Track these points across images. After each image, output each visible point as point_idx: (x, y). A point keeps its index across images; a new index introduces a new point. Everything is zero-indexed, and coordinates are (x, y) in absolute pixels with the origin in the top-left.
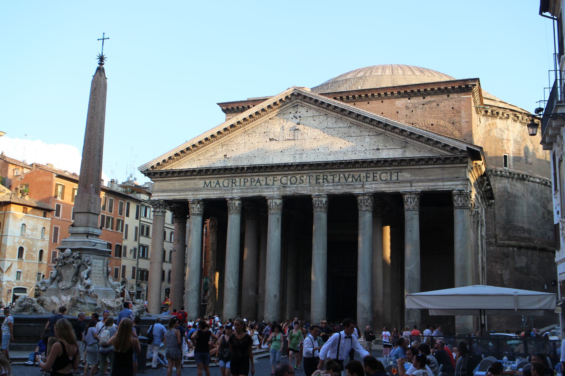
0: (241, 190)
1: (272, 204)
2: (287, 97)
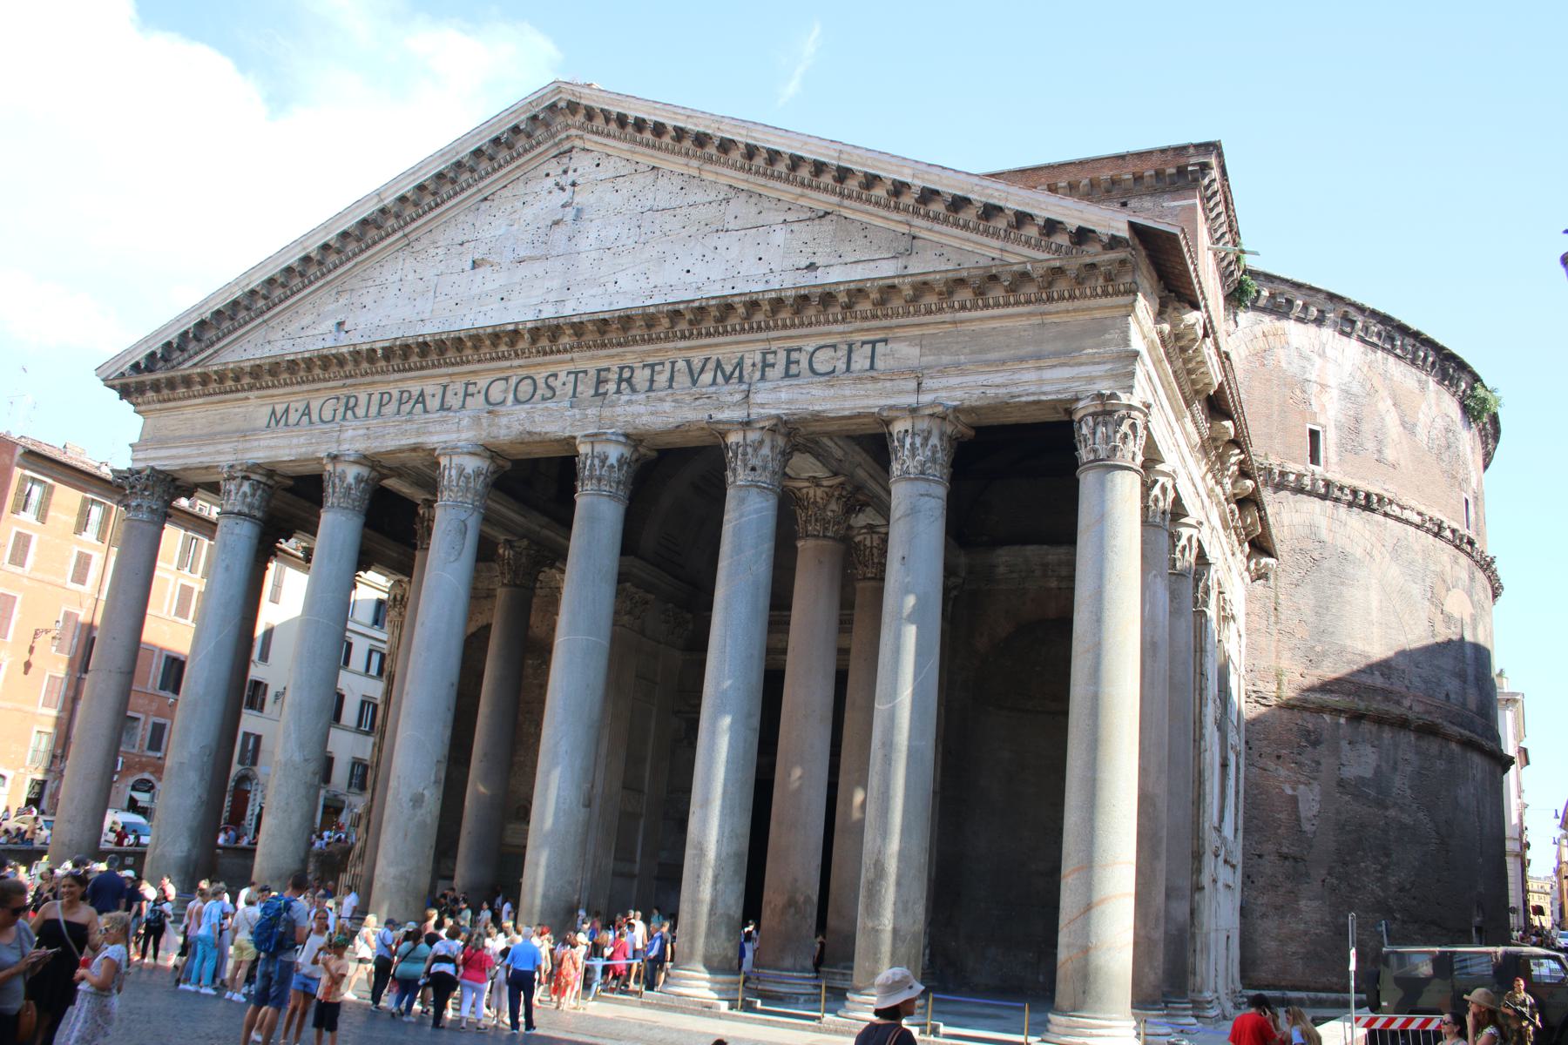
0: (365, 431)
1: (447, 472)
2: (534, 118)
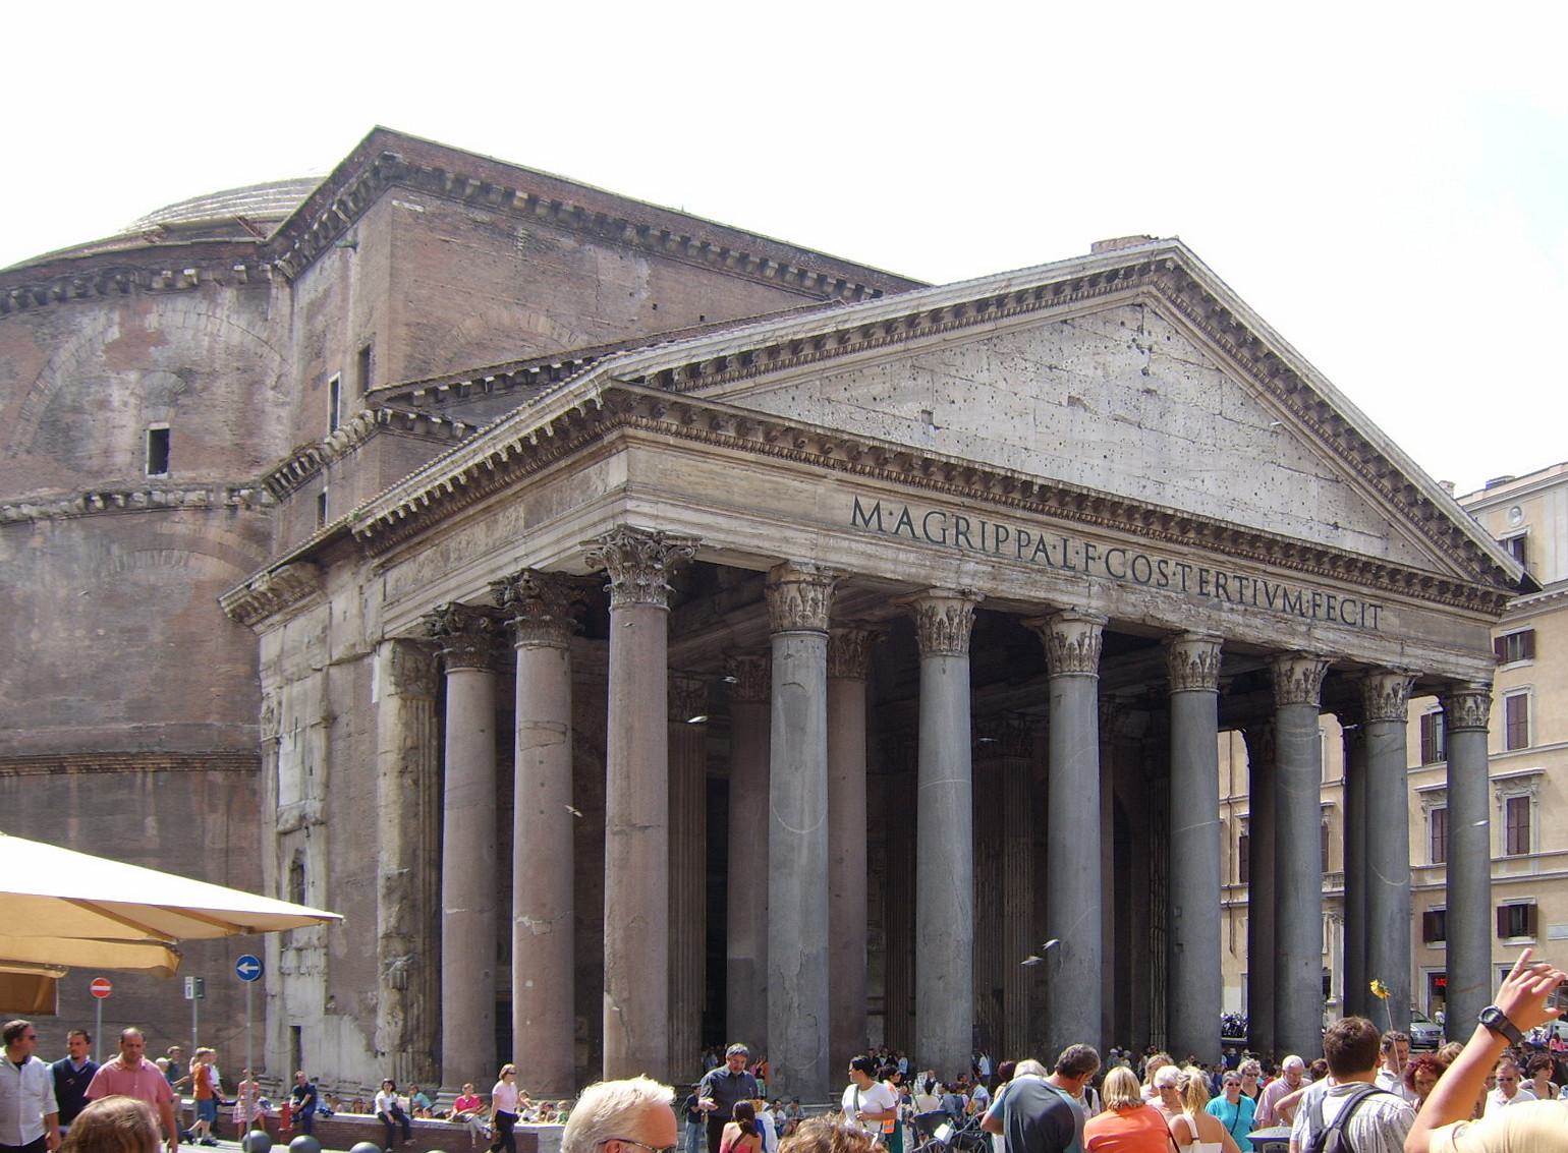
0: (990, 569)
1: (1087, 641)
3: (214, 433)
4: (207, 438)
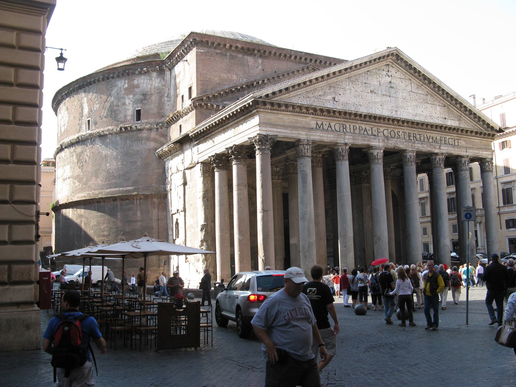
0: (352, 137)
1: (379, 154)
3: (152, 110)
4: (150, 111)
